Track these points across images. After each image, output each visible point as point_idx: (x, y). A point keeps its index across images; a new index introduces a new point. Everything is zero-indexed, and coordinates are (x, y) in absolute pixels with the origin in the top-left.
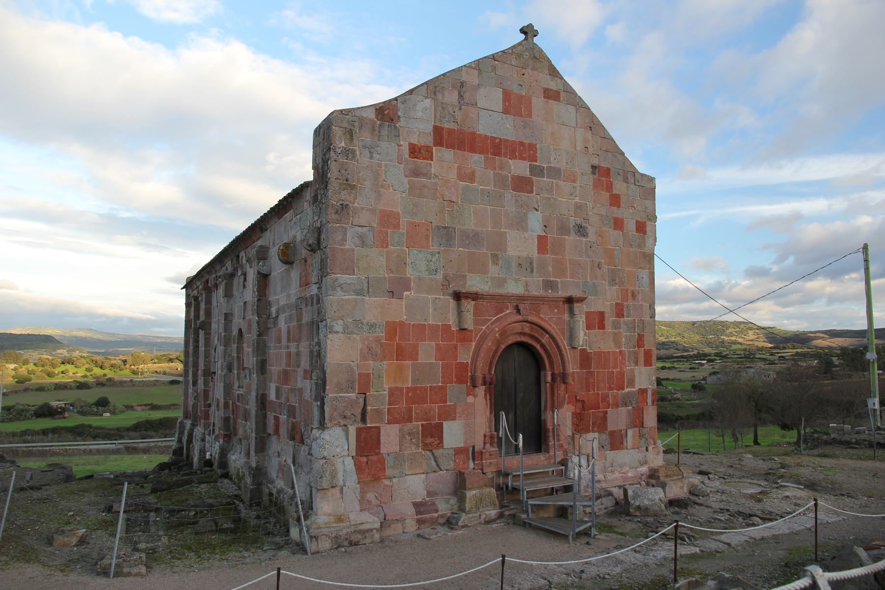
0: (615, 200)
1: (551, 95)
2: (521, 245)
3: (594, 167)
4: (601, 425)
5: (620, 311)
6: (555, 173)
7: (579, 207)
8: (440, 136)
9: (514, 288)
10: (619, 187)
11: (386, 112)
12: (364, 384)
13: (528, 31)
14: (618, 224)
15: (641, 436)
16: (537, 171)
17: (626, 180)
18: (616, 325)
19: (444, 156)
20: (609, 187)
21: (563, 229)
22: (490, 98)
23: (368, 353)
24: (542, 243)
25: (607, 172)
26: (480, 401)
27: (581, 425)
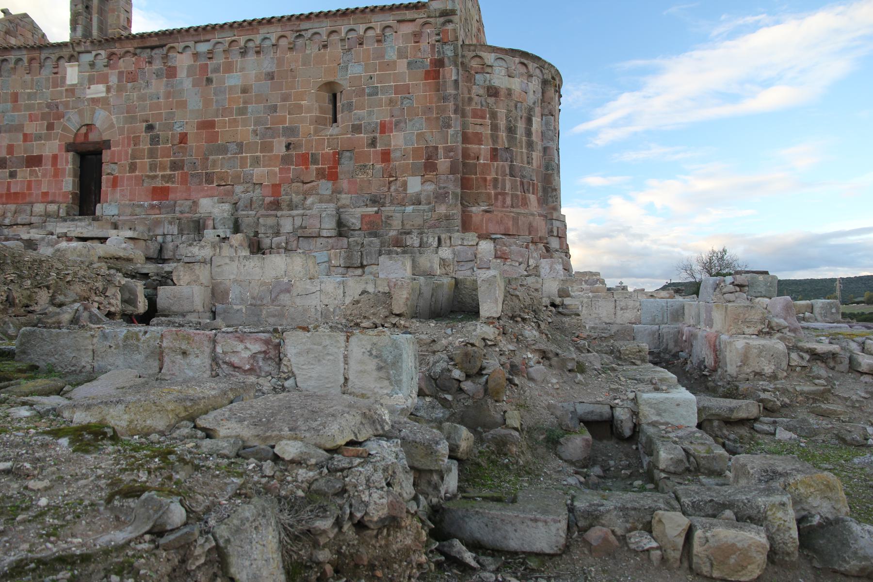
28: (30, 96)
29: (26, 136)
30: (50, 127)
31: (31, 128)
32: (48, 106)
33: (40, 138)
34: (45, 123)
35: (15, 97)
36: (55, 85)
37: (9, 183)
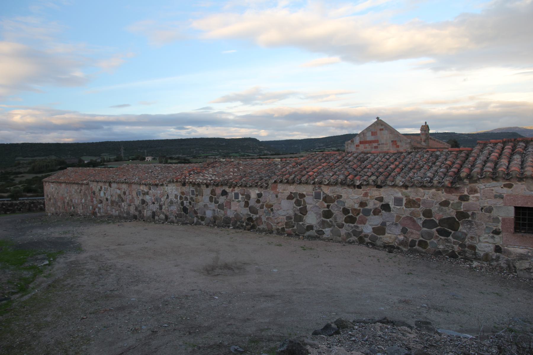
0: (398, 146)
1: (381, 130)
3: (392, 141)
6: (383, 144)
8: (361, 143)
10: (399, 143)
13: (378, 118)
17: (401, 142)
20: (396, 144)
22: (369, 134)
25: (395, 141)
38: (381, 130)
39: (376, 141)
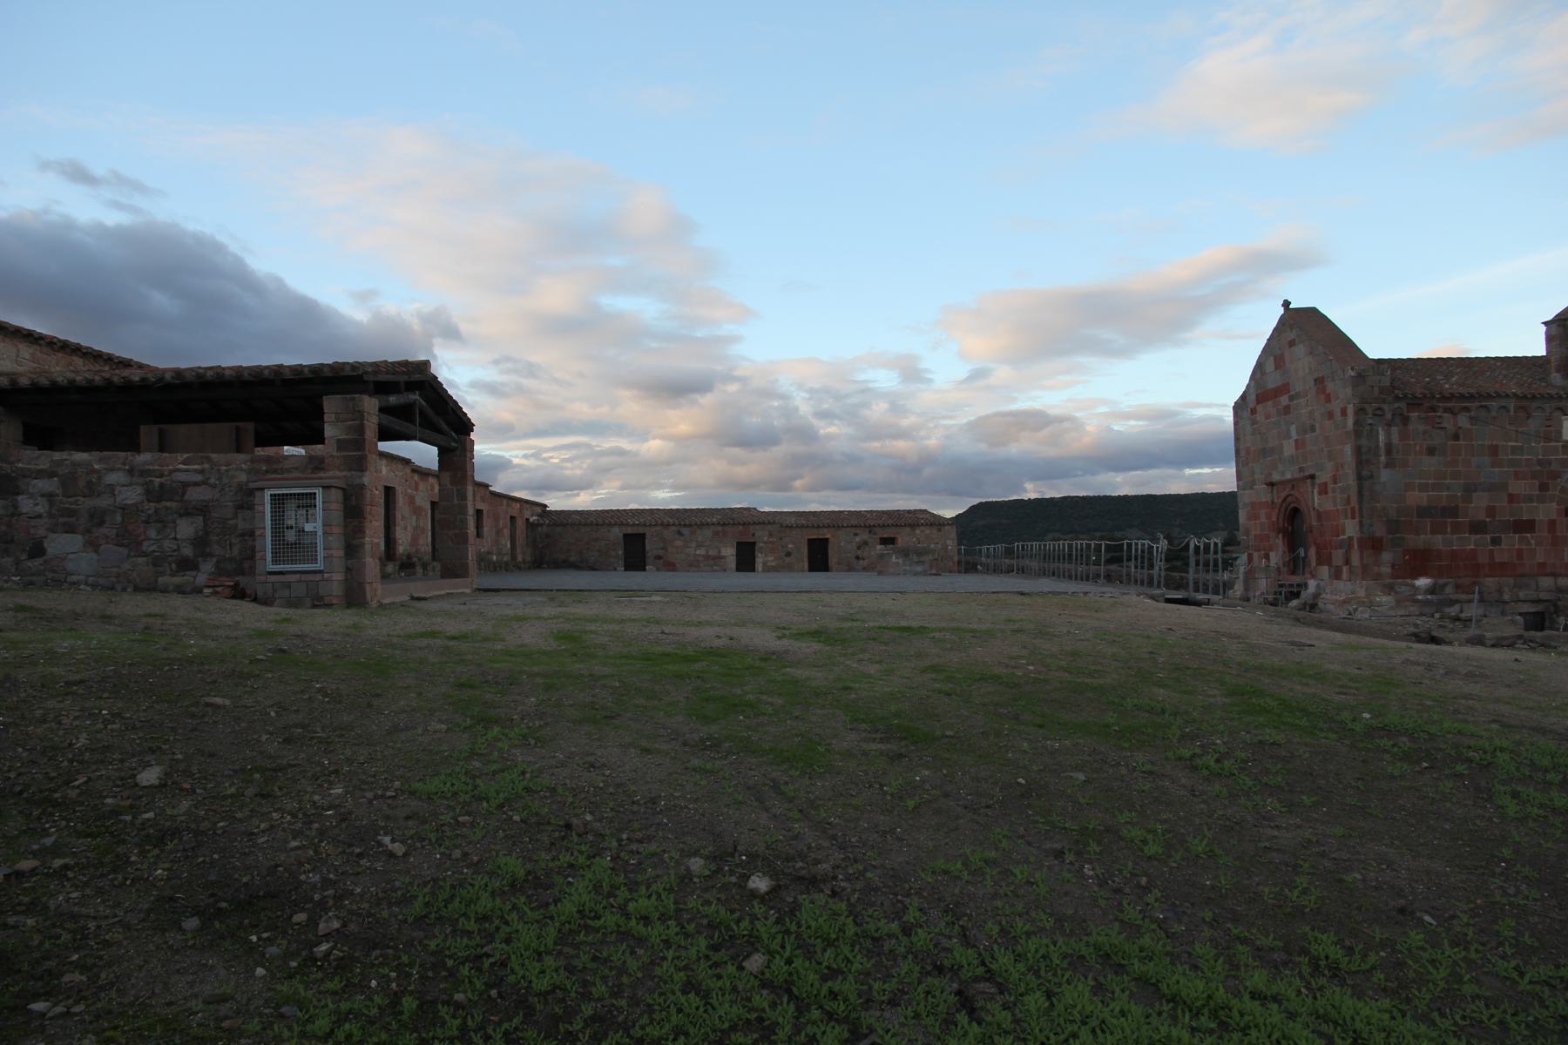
2: (1289, 449)
4: (1329, 562)
5: (1335, 480)
7: (1311, 412)
9: (1288, 476)
10: (1330, 387)
11: (1243, 397)
12: (1247, 533)
13: (1286, 304)
14: (1330, 415)
15: (1351, 572)
16: (1291, 398)
18: (1334, 491)
19: (1260, 408)
20: (1324, 388)
21: (1305, 432)
23: (1249, 519)
24: (1299, 444)
26: (1279, 542)
27: (1320, 562)
28: (1514, 450)
29: (1512, 498)
30: (1543, 487)
31: (1518, 487)
32: (1540, 462)
33: (1530, 499)
34: (1537, 482)
35: (1494, 451)
36: (1548, 439)
37: (1491, 552)
38: (1292, 343)
39: (1283, 389)
